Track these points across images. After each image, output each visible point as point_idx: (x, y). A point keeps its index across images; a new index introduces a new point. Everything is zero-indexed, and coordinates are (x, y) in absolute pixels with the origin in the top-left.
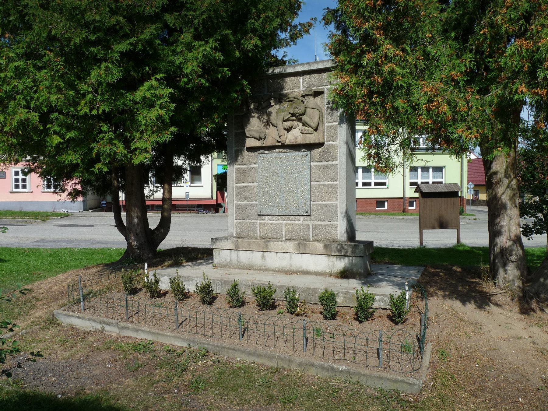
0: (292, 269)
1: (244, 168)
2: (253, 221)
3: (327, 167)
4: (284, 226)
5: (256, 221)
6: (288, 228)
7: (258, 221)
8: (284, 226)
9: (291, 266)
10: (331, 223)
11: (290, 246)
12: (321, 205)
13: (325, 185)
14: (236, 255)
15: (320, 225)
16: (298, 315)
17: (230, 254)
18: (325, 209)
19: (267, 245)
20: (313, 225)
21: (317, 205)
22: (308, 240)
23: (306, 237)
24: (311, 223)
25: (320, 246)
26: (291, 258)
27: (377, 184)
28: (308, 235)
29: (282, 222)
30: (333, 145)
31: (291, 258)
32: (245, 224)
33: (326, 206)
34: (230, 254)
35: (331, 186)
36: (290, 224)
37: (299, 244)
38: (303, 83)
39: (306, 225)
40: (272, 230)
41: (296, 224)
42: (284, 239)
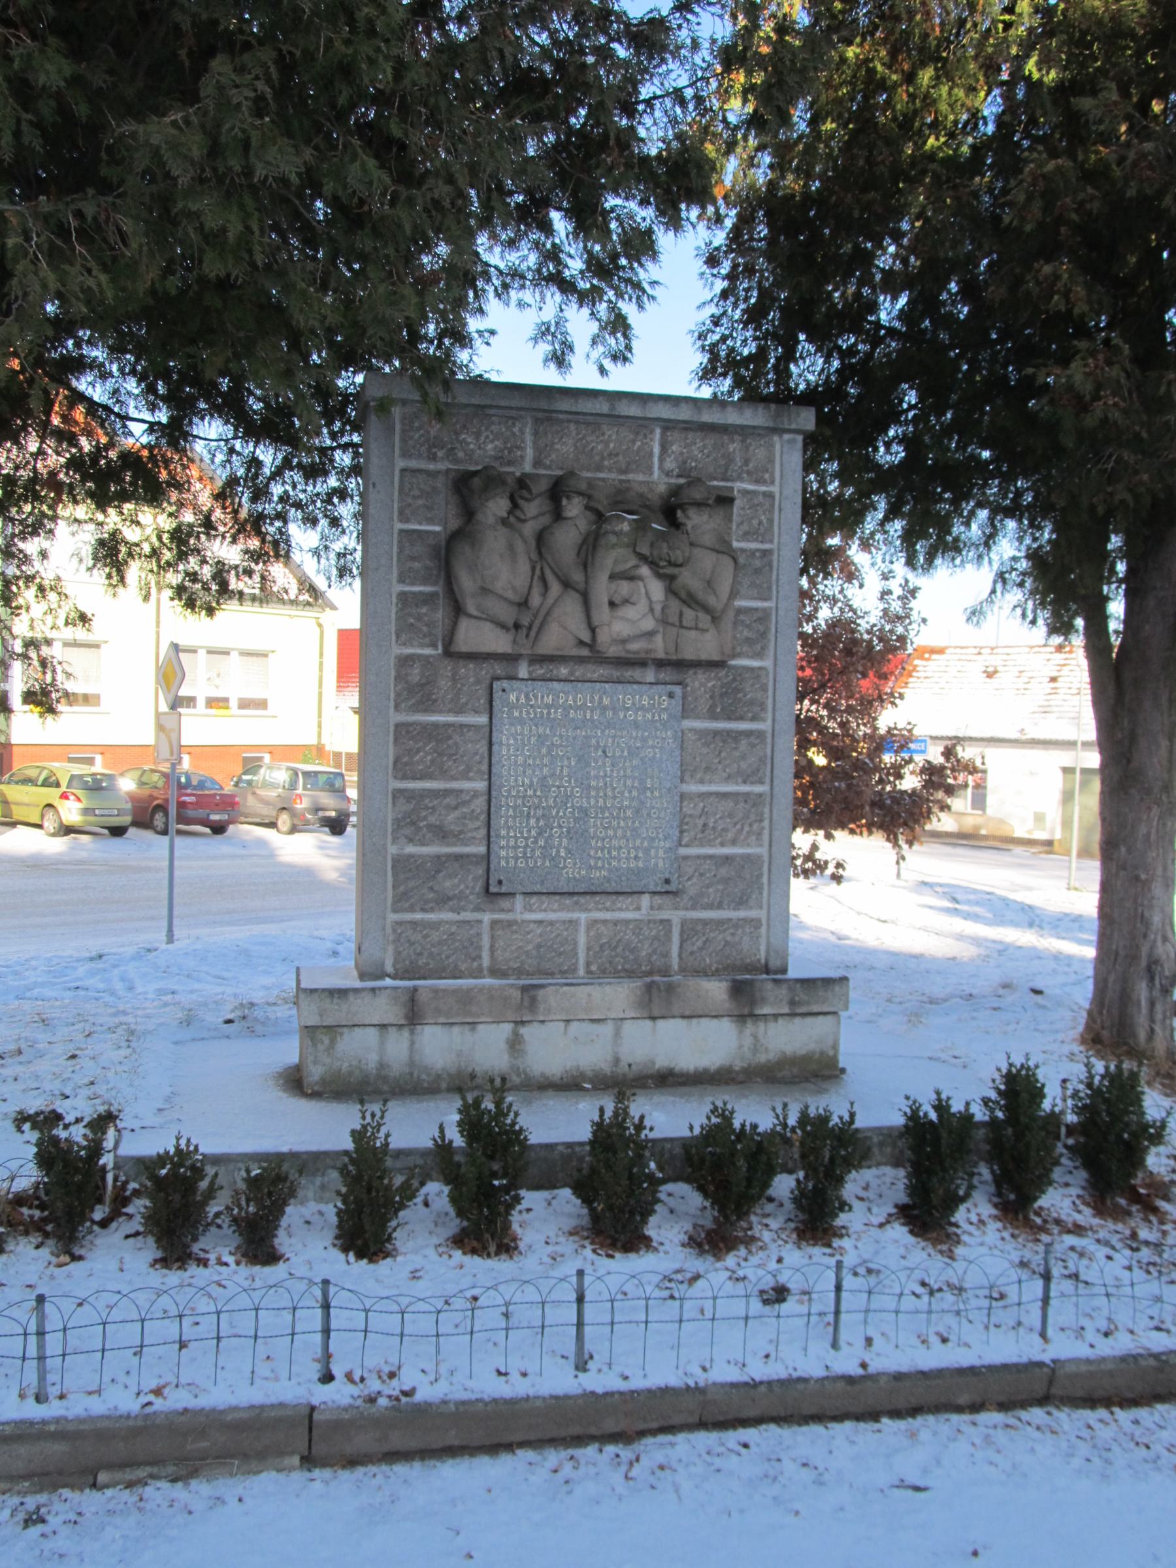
0: (623, 1068)
1: (436, 725)
2: (467, 915)
3: (737, 736)
4: (582, 929)
5: (477, 916)
6: (599, 936)
7: (487, 918)
8: (582, 929)
9: (617, 1060)
10: (742, 914)
11: (619, 995)
12: (711, 857)
13: (724, 796)
14: (405, 1044)
15: (705, 923)
16: (1098, 1241)
17: (382, 1043)
18: (723, 872)
19: (533, 1001)
20: (684, 923)
21: (698, 857)
22: (665, 972)
23: (658, 962)
24: (676, 917)
25: (716, 990)
26: (617, 1034)
27: (245, 704)
28: (666, 955)
29: (575, 915)
30: (752, 669)
31: (617, 1034)
32: (435, 925)
33: (727, 859)
34: (382, 1043)
35: (746, 796)
36: (605, 922)
37: (649, 987)
38: (661, 460)
39: (662, 921)
40: (539, 946)
41: (627, 922)
42: (581, 972)
